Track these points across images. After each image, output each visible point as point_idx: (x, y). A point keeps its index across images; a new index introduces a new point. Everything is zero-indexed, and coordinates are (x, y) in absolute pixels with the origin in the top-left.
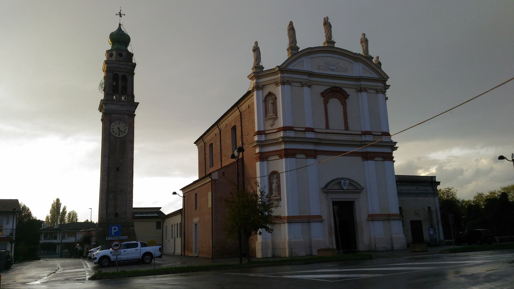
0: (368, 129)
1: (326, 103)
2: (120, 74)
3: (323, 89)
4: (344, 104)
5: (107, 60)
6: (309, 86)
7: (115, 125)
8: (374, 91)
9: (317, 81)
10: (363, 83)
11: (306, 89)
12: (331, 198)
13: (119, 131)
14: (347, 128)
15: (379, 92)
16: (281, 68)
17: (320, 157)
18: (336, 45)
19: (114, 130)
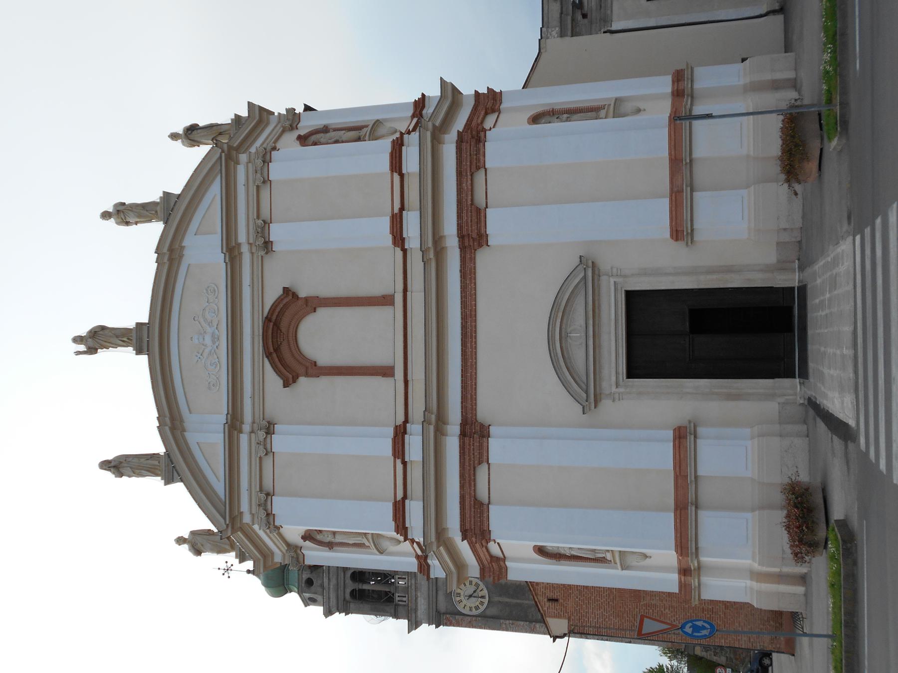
0: (385, 223)
1: (314, 370)
2: (351, 586)
3: (273, 380)
4: (313, 304)
5: (323, 606)
6: (269, 430)
7: (462, 605)
8: (265, 194)
9: (253, 397)
10: (242, 237)
11: (278, 443)
12: (617, 386)
13: (474, 597)
14: (386, 300)
15: (266, 179)
16: (225, 526)
17: (485, 410)
18: (145, 319)
19: (473, 605)
